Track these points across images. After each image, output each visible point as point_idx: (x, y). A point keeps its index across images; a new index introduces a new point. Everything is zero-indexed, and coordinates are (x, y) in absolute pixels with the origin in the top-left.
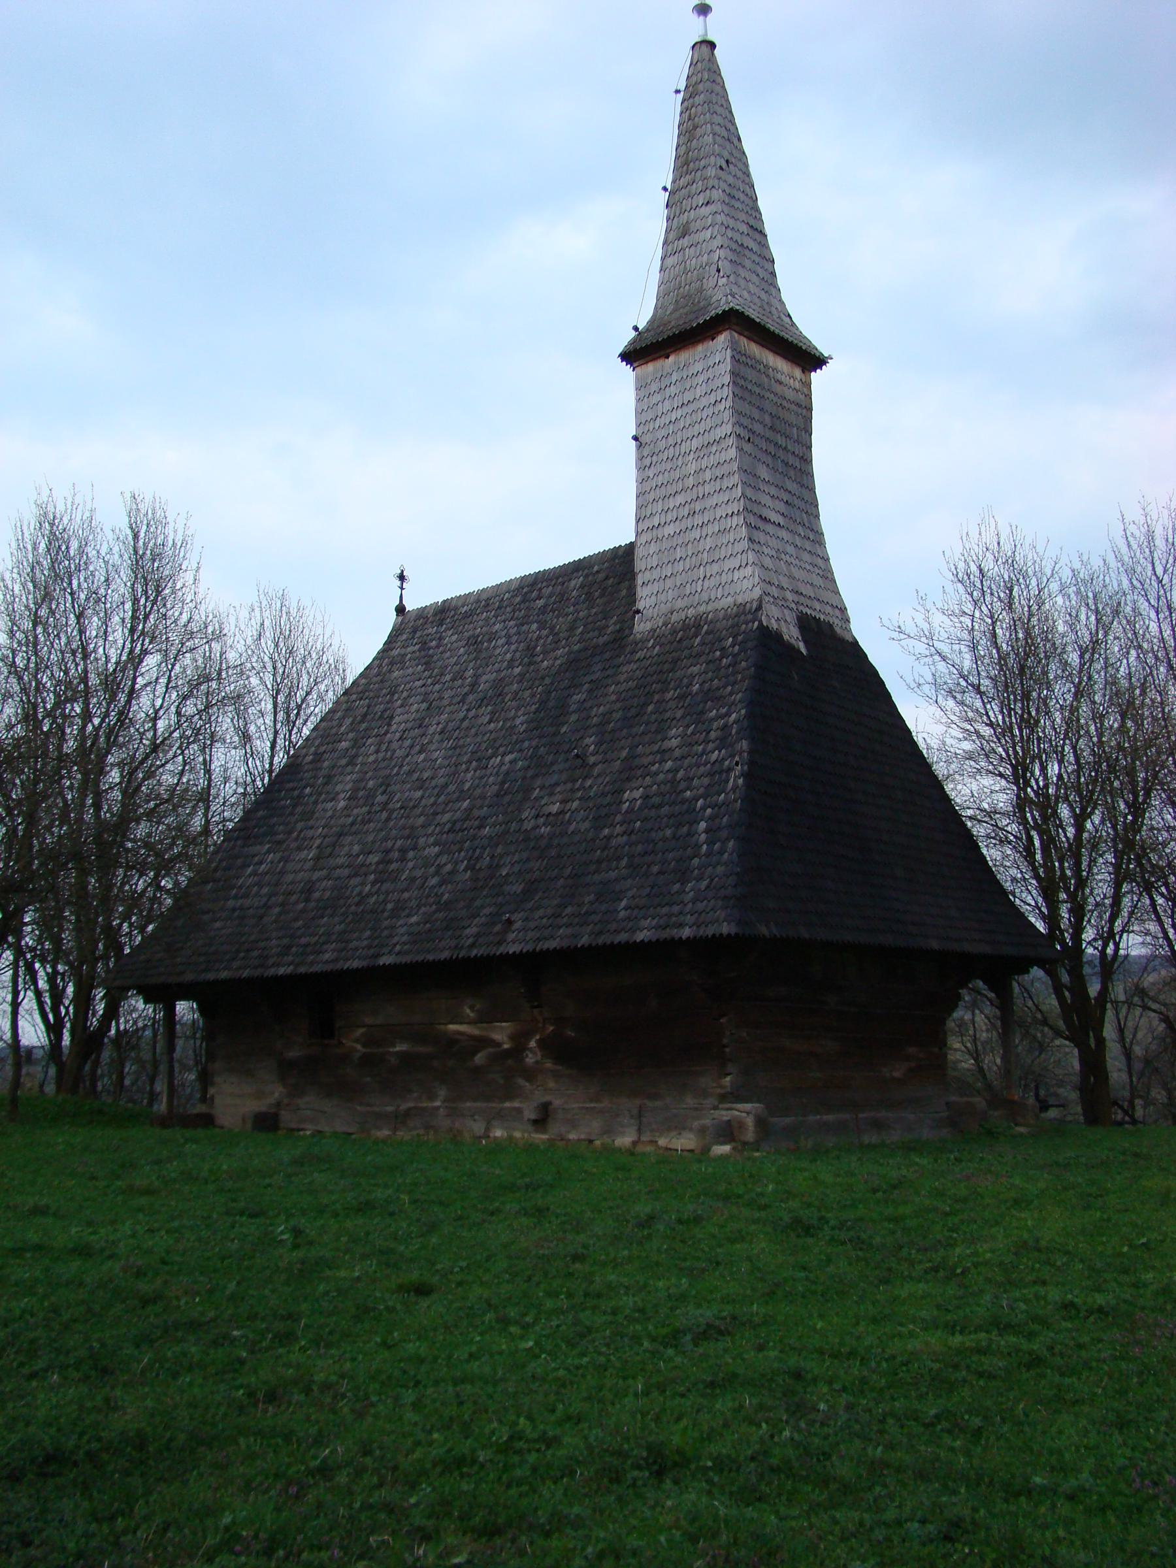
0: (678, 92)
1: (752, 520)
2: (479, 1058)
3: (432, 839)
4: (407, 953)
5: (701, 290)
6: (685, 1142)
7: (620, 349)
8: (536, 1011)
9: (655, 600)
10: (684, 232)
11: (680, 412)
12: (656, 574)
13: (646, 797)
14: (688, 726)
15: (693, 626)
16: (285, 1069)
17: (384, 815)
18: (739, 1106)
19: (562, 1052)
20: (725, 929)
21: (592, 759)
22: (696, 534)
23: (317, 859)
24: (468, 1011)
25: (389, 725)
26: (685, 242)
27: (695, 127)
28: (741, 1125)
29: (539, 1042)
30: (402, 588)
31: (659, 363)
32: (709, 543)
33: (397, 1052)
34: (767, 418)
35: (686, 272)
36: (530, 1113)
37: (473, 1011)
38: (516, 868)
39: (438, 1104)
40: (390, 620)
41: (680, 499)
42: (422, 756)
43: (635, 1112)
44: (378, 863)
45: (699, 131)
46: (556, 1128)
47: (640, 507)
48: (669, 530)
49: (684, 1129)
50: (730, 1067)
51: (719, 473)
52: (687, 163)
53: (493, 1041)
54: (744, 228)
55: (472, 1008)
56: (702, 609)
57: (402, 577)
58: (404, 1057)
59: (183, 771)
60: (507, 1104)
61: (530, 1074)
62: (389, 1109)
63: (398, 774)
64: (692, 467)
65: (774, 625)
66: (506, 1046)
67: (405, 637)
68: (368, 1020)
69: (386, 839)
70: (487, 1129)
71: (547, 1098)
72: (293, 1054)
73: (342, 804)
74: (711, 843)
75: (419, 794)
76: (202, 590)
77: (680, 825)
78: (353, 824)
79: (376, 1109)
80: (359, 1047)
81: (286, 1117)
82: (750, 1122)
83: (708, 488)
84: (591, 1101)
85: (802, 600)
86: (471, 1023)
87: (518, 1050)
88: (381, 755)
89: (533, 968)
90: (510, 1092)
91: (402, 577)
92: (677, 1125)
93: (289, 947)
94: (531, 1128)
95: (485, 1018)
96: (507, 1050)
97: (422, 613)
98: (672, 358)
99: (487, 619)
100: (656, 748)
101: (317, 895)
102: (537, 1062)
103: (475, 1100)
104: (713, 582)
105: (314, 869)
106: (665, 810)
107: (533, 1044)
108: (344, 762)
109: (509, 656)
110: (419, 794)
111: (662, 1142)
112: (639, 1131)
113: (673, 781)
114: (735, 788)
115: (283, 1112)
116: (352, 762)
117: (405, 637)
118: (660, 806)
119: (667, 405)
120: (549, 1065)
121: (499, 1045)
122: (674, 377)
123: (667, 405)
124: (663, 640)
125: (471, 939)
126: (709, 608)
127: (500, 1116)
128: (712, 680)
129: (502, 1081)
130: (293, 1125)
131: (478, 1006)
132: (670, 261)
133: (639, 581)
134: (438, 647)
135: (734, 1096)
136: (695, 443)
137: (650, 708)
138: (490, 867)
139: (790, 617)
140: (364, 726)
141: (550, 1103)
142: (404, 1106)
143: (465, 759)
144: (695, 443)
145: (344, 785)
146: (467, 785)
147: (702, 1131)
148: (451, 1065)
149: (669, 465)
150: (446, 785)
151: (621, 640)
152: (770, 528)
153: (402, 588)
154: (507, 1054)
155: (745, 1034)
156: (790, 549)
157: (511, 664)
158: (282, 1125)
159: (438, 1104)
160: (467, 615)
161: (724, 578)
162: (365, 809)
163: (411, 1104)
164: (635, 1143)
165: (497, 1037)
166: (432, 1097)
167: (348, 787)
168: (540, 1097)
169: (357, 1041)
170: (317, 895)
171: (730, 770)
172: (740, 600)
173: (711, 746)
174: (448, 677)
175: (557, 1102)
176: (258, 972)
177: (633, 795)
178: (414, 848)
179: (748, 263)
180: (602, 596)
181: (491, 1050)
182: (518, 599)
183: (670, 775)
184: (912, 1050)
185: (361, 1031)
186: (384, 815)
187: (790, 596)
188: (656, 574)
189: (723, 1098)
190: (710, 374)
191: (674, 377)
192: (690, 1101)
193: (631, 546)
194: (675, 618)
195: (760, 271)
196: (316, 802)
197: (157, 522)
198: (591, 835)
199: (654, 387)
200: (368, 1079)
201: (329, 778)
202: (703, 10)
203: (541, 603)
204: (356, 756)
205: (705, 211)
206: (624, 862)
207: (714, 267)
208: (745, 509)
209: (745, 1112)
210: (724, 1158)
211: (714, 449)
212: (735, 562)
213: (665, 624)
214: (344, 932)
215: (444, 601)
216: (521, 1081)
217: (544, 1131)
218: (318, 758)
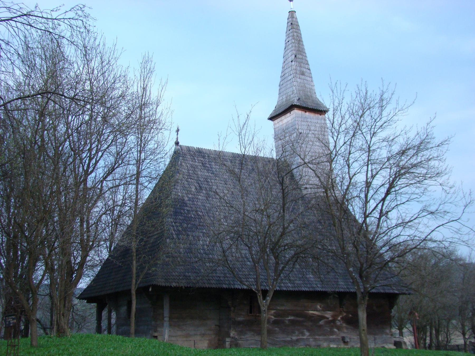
2: (322, 322)
24: (319, 307)
29: (342, 318)
31: (303, 113)
33: (289, 320)
37: (320, 307)
43: (373, 339)
60: (331, 337)
62: (289, 339)
66: (330, 319)
68: (278, 308)
71: (344, 335)
72: (240, 319)
80: (273, 317)
87: (334, 321)
90: (332, 333)
95: (325, 309)
96: (24, 328)
98: (307, 113)
120: (344, 325)
121: (328, 318)
127: (333, 341)
129: (329, 330)
142: (294, 338)
154: (331, 321)
159: (305, 337)
165: (327, 316)
166: (303, 334)
169: (272, 315)
200: (276, 329)
216: (336, 330)
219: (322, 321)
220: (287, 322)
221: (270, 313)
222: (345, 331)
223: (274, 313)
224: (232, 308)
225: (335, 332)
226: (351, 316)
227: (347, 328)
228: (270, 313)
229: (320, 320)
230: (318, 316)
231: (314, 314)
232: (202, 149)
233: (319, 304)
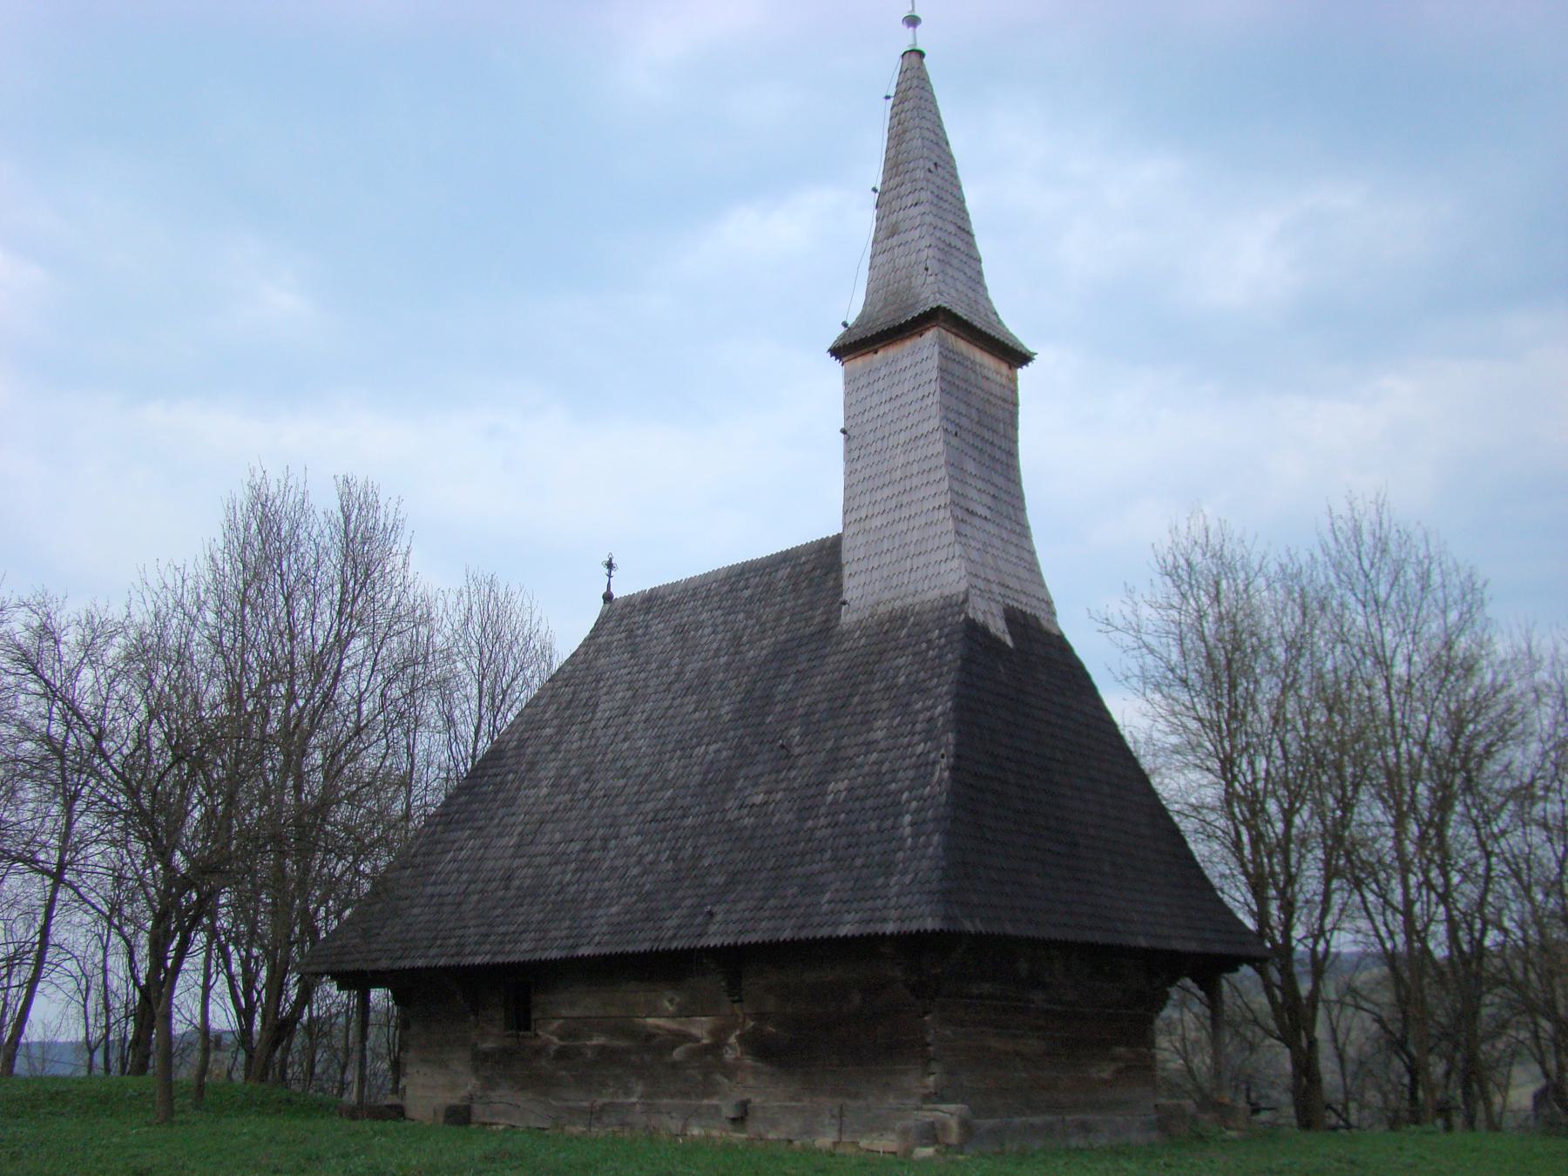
0: (887, 98)
1: (959, 513)
2: (678, 1054)
3: (634, 829)
4: (607, 943)
5: (909, 288)
6: (886, 1143)
7: (829, 345)
8: (736, 1006)
9: (863, 593)
10: (893, 232)
11: (887, 407)
12: (863, 565)
13: (850, 790)
14: (894, 718)
15: (899, 618)
16: (480, 1060)
17: (587, 802)
18: (943, 1107)
19: (763, 1049)
20: (931, 924)
21: (797, 751)
22: (903, 526)
23: (518, 846)
24: (667, 1004)
25: (594, 712)
26: (895, 241)
27: (905, 132)
28: (945, 1127)
29: (740, 1038)
30: (610, 576)
32: (916, 535)
34: (974, 415)
35: (895, 270)
36: (729, 1111)
38: (719, 859)
39: (634, 1100)
40: (598, 606)
41: (887, 492)
42: (626, 745)
43: (836, 1111)
44: (579, 852)
45: (908, 136)
46: (754, 1127)
47: (847, 500)
48: (877, 522)
49: (886, 1129)
50: (935, 1067)
51: (925, 466)
52: (896, 166)
54: (952, 229)
55: (671, 1001)
56: (909, 600)
57: (610, 565)
58: (602, 1050)
60: (705, 1102)
61: (730, 1071)
63: (601, 761)
64: (900, 460)
65: (980, 618)
66: (705, 1041)
67: (612, 624)
68: (564, 1012)
69: (588, 827)
70: (684, 1127)
71: (746, 1096)
72: (488, 1045)
73: (545, 791)
74: (915, 836)
75: (622, 782)
76: (411, 574)
77: (886, 817)
78: (554, 812)
79: (571, 1104)
80: (555, 1040)
81: (477, 1109)
82: (953, 1124)
83: (915, 481)
84: (792, 1099)
85: (1009, 593)
86: (672, 1017)
87: (717, 1047)
88: (585, 743)
89: (734, 962)
90: (709, 1089)
91: (610, 565)
92: (878, 1126)
93: (488, 935)
94: (729, 1126)
95: (685, 1012)
97: (629, 602)
98: (881, 353)
99: (695, 608)
100: (861, 739)
101: (517, 883)
102: (737, 1059)
103: (672, 1096)
104: (920, 574)
105: (514, 856)
106: (869, 803)
107: (732, 1040)
108: (547, 748)
109: (715, 645)
110: (622, 782)
111: (864, 1143)
112: (840, 1131)
113: (878, 774)
114: (939, 783)
115: (475, 1106)
116: (555, 749)
117: (612, 624)
118: (865, 798)
119: (876, 400)
120: (748, 1061)
121: (697, 1040)
122: (883, 372)
123: (876, 400)
124: (870, 632)
125: (671, 933)
126: (917, 600)
128: (918, 672)
130: (486, 1120)
131: (678, 999)
132: (879, 260)
133: (846, 571)
134: (644, 635)
135: (939, 1097)
136: (903, 437)
137: (856, 699)
138: (692, 857)
139: (997, 610)
140: (569, 712)
141: (749, 1101)
142: (600, 1101)
143: (670, 747)
144: (903, 437)
145: (548, 771)
146: (671, 774)
147: (905, 1132)
148: (647, 1057)
149: (877, 458)
150: (649, 775)
151: (827, 631)
152: (977, 522)
153: (610, 576)
154: (707, 1049)
155: (948, 1032)
156: (997, 543)
157: (717, 654)
158: (474, 1119)
159: (634, 1100)
160: (676, 604)
161: (931, 571)
162: (568, 797)
163: (606, 1100)
164: (835, 1144)
165: (695, 1031)
166: (628, 1093)
167: (552, 773)
168: (738, 1095)
169: (553, 1033)
170: (517, 883)
171: (935, 762)
172: (947, 592)
173: (917, 738)
174: (654, 666)
175: (757, 1100)
176: (453, 961)
177: (838, 786)
178: (617, 837)
179: (955, 262)
180: (809, 586)
181: (690, 1045)
182: (726, 588)
183: (875, 768)
184: (1120, 1050)
185: (556, 1024)
186: (587, 802)
187: (995, 588)
188: (863, 565)
189: (926, 1098)
190: (918, 369)
191: (883, 372)
192: (892, 1101)
193: (836, 542)
194: (881, 609)
195: (967, 270)
196: (518, 789)
197: (368, 505)
198: (795, 826)
199: (863, 381)
201: (532, 765)
202: (912, 21)
203: (747, 593)
204: (559, 743)
205: (915, 211)
206: (828, 855)
207: (922, 266)
208: (952, 502)
209: (949, 1114)
210: (927, 1160)
211: (921, 442)
212: (941, 555)
213: (872, 616)
214: (543, 921)
215: (652, 590)
216: (719, 1077)
217: (743, 1131)
218: (522, 743)
220: (589, 1054)
222: (751, 1081)
223: (559, 1027)
229: (674, 1048)
230: (669, 1031)
231: (658, 1027)
233: (669, 994)
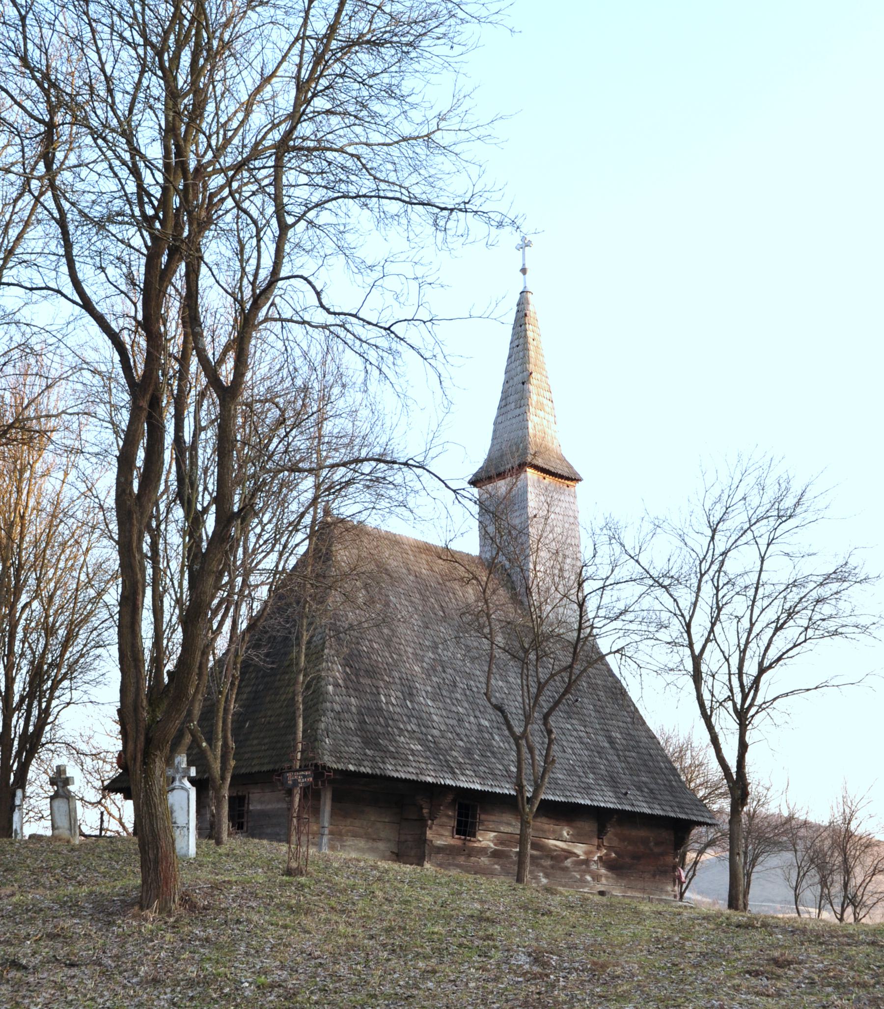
2: (568, 863)
24: (565, 833)
53: (575, 854)
59: (107, 527)
66: (581, 857)
68: (502, 829)
89: (601, 818)
95: (577, 838)
120: (603, 871)
121: (578, 856)
129: (579, 877)
132: (495, 442)
165: (576, 851)
200: (496, 866)
219: (569, 860)
221: (487, 837)
223: (495, 837)
224: (430, 822)
225: (588, 882)
226: (614, 855)
227: (607, 877)
228: (487, 837)
229: (567, 858)
230: (563, 850)
231: (556, 846)
232: (395, 535)
